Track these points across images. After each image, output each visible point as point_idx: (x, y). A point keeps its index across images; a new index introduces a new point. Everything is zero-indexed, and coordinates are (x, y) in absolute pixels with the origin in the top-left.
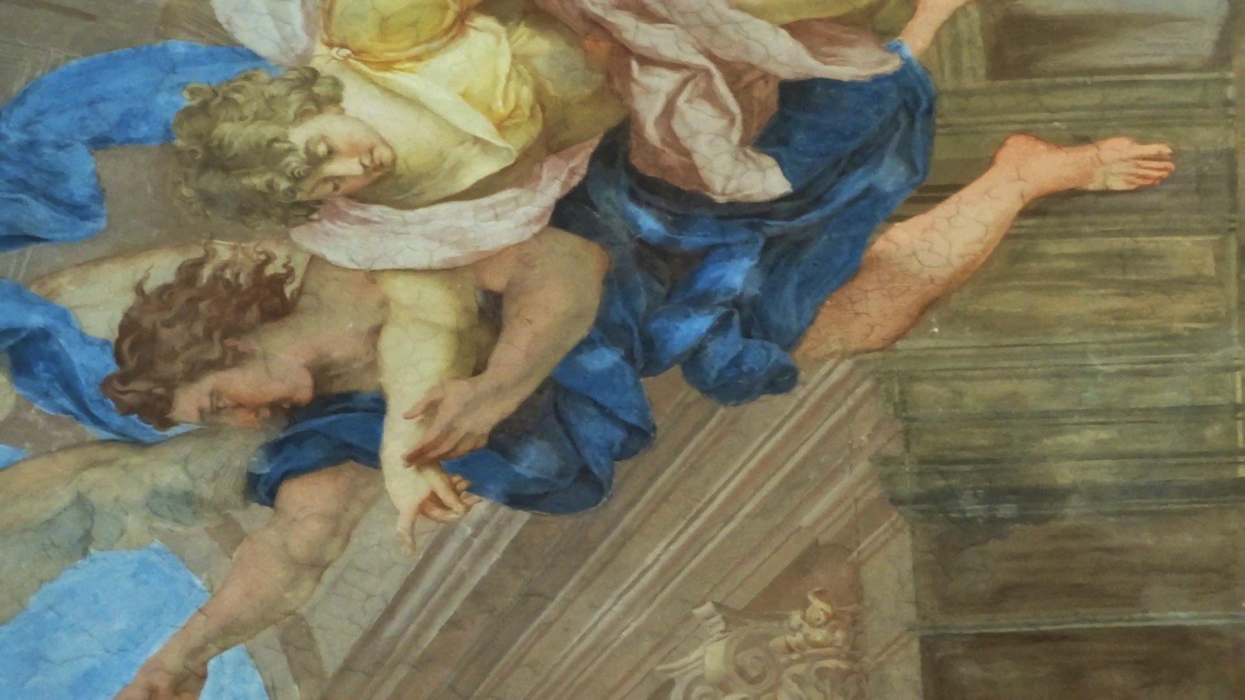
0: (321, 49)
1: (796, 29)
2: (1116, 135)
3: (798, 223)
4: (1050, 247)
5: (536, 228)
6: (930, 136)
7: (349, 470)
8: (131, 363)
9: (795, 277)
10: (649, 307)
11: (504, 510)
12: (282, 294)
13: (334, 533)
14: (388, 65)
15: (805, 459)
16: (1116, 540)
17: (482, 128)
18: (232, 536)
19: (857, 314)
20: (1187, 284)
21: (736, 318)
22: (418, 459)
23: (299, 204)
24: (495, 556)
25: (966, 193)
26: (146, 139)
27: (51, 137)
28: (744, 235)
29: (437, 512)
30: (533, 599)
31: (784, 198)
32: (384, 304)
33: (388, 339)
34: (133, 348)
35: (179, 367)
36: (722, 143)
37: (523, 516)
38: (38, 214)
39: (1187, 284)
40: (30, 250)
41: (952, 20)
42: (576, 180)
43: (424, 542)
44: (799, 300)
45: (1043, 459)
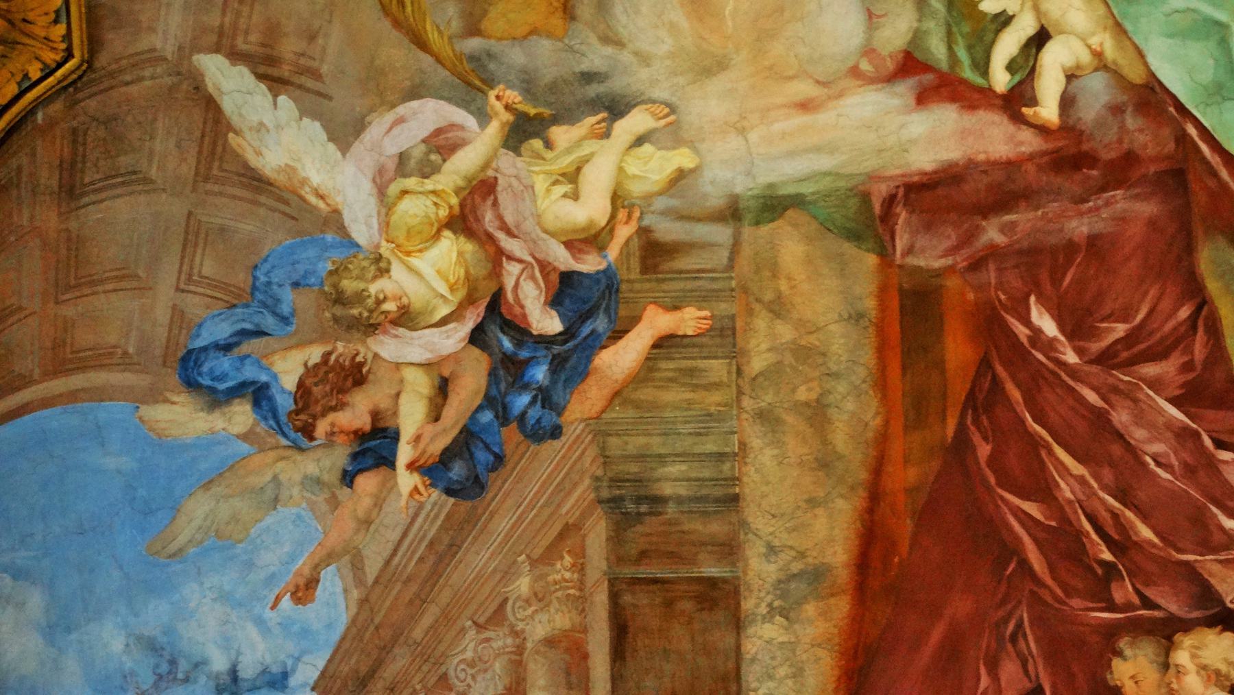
0: (384, 243)
1: (568, 245)
2: (687, 306)
3: (566, 347)
4: (663, 365)
5: (463, 344)
6: (617, 302)
7: (383, 471)
8: (300, 405)
9: (563, 377)
10: (506, 388)
11: (444, 497)
12: (360, 371)
13: (375, 505)
14: (408, 254)
15: (563, 480)
16: (686, 527)
17: (443, 289)
18: (334, 503)
19: (587, 398)
20: (717, 386)
21: (540, 397)
22: (411, 466)
23: (371, 325)
24: (439, 522)
25: (631, 335)
26: (314, 285)
27: (276, 280)
28: (544, 352)
29: (417, 497)
30: (454, 547)
31: (560, 334)
32: (402, 381)
33: (403, 399)
34: (301, 397)
35: (319, 408)
36: (536, 301)
37: (452, 500)
38: (269, 322)
39: (717, 386)
40: (265, 339)
41: (627, 243)
42: (480, 319)
43: (411, 511)
44: (565, 388)
45: (659, 480)
